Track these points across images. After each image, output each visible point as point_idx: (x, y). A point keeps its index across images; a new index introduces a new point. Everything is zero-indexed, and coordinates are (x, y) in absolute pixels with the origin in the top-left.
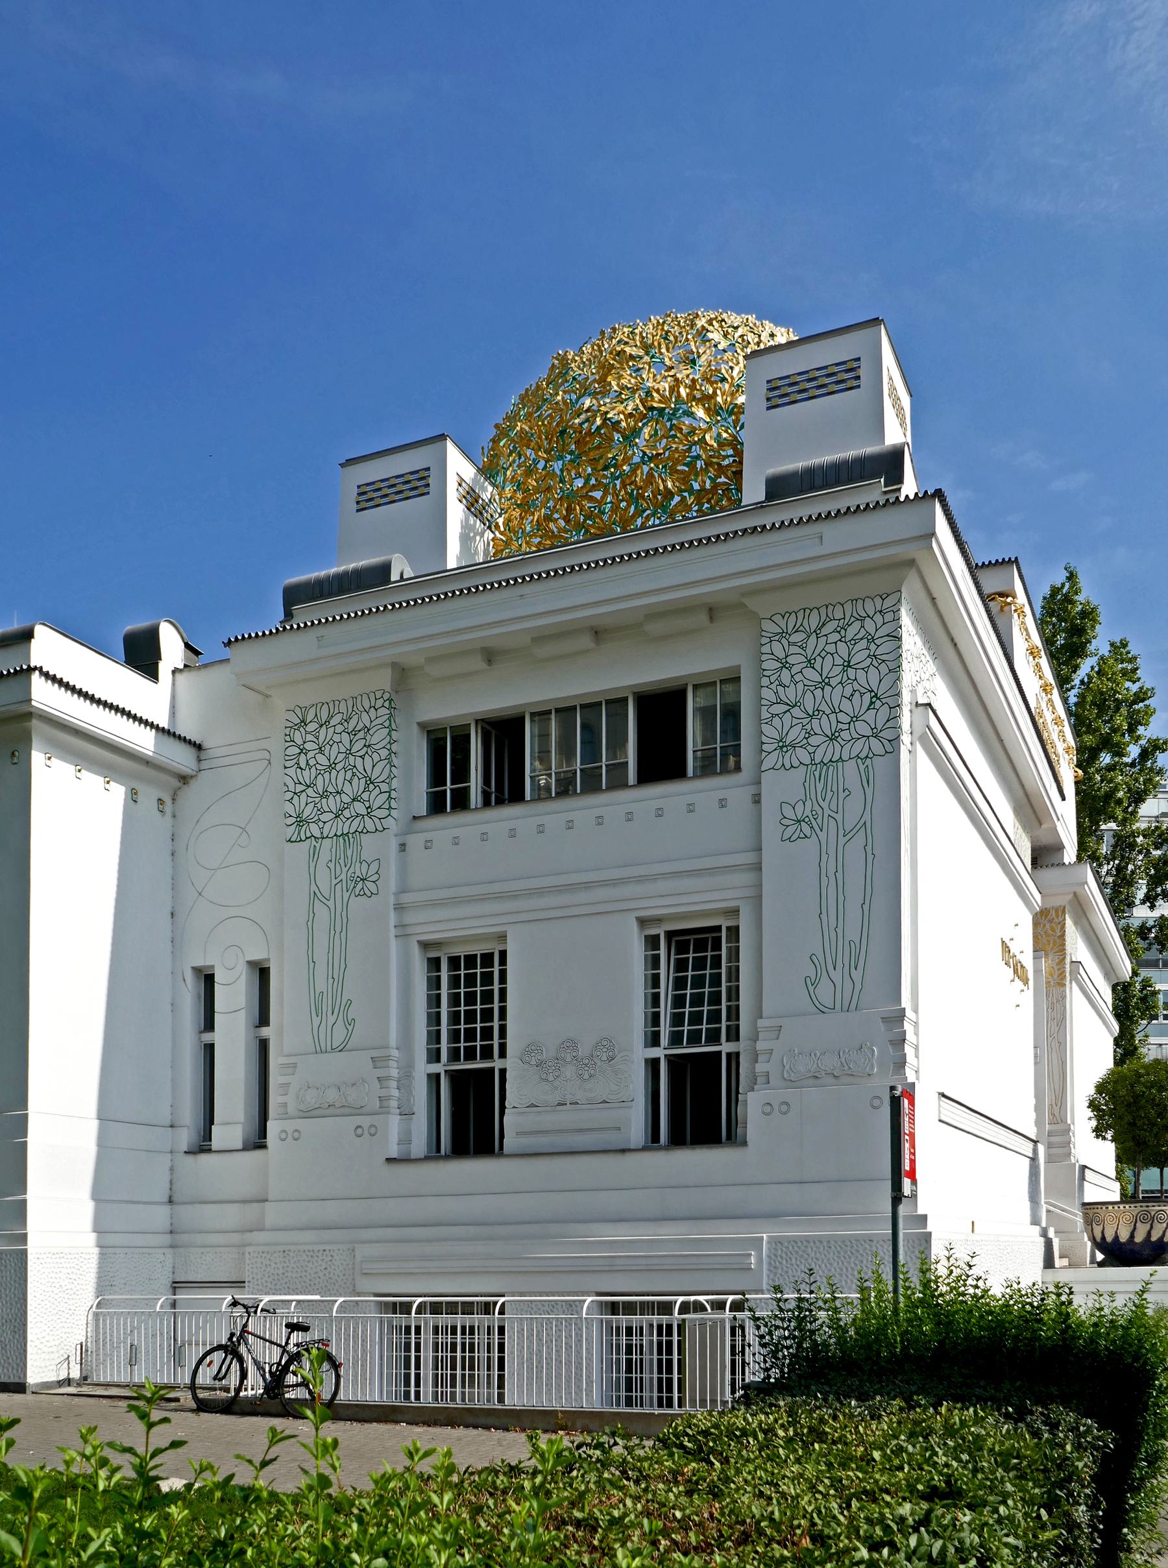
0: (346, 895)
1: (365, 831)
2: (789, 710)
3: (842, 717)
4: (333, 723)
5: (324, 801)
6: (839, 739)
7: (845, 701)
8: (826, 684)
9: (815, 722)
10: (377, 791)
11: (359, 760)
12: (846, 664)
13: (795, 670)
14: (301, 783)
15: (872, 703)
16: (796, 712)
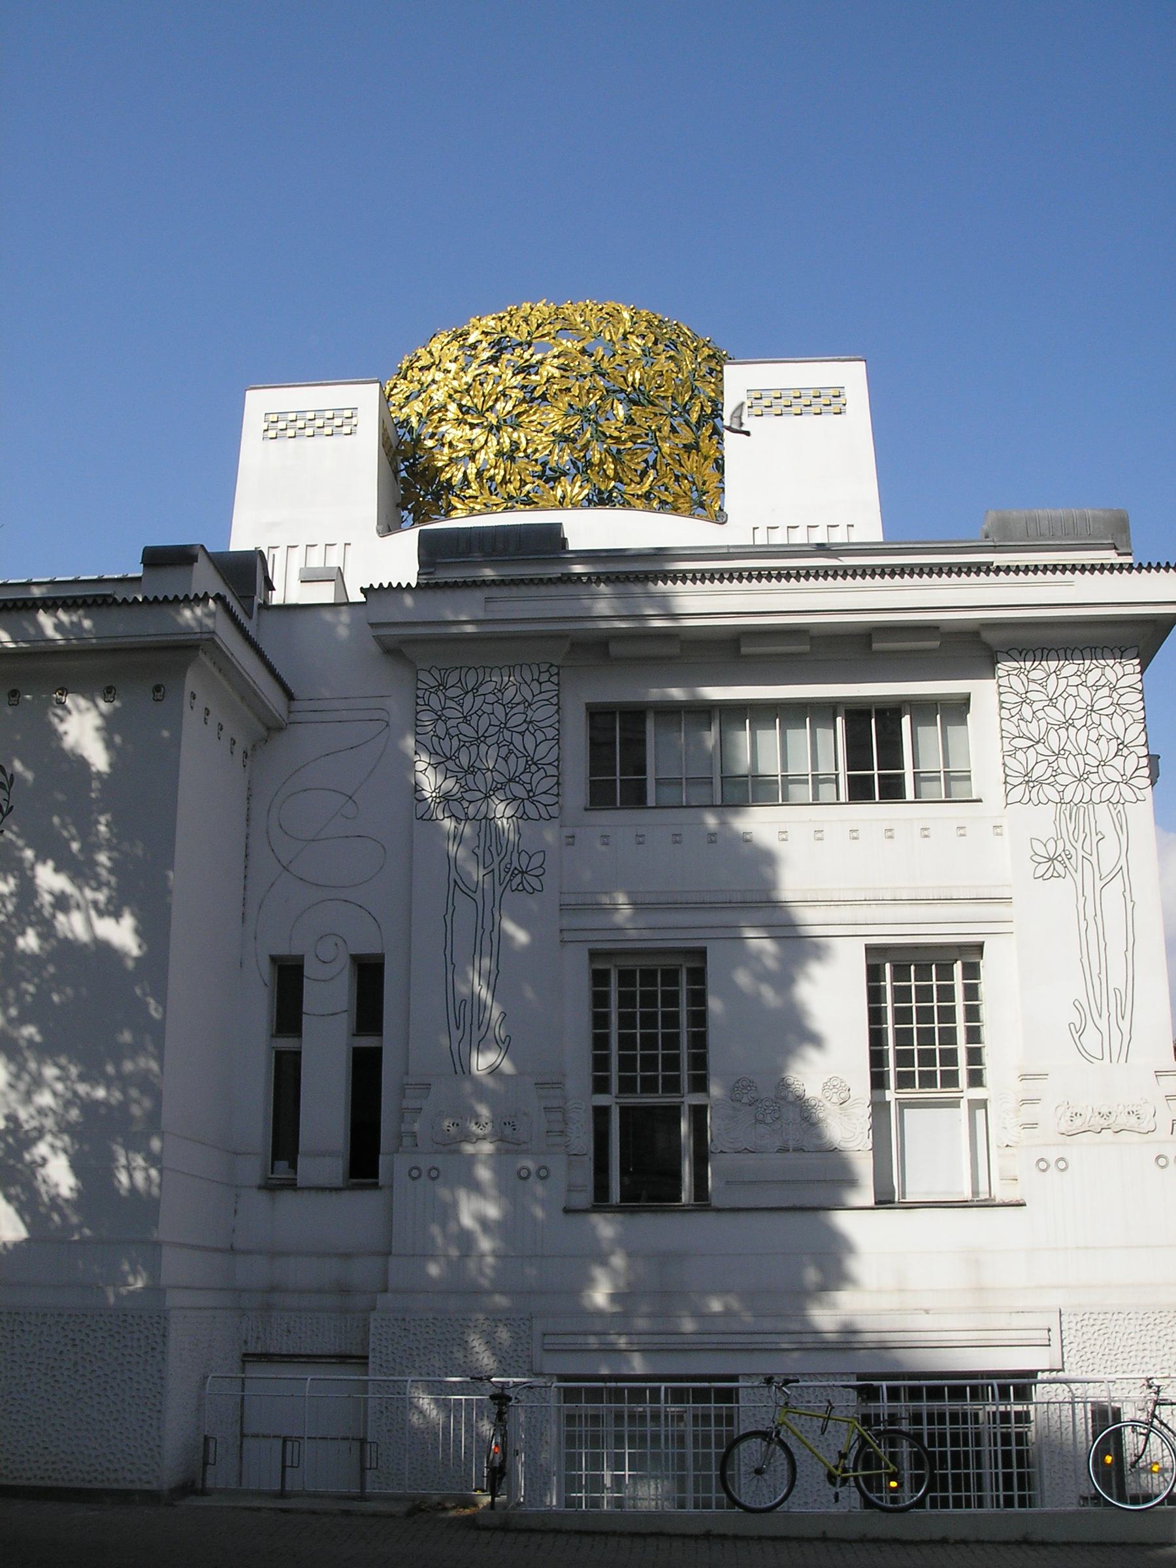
0: (499, 890)
1: (525, 817)
2: (1032, 746)
3: (1088, 759)
4: (481, 691)
5: (470, 777)
6: (1088, 781)
7: (1091, 745)
8: (1070, 724)
9: (1062, 762)
10: (541, 773)
11: (516, 736)
12: (1089, 708)
13: (1036, 706)
14: (437, 754)
15: (1118, 750)
16: (1040, 748)
